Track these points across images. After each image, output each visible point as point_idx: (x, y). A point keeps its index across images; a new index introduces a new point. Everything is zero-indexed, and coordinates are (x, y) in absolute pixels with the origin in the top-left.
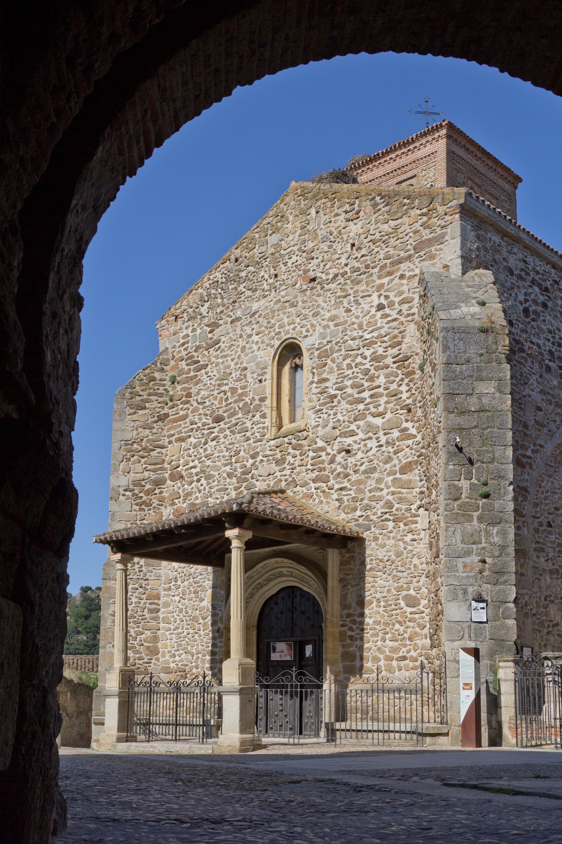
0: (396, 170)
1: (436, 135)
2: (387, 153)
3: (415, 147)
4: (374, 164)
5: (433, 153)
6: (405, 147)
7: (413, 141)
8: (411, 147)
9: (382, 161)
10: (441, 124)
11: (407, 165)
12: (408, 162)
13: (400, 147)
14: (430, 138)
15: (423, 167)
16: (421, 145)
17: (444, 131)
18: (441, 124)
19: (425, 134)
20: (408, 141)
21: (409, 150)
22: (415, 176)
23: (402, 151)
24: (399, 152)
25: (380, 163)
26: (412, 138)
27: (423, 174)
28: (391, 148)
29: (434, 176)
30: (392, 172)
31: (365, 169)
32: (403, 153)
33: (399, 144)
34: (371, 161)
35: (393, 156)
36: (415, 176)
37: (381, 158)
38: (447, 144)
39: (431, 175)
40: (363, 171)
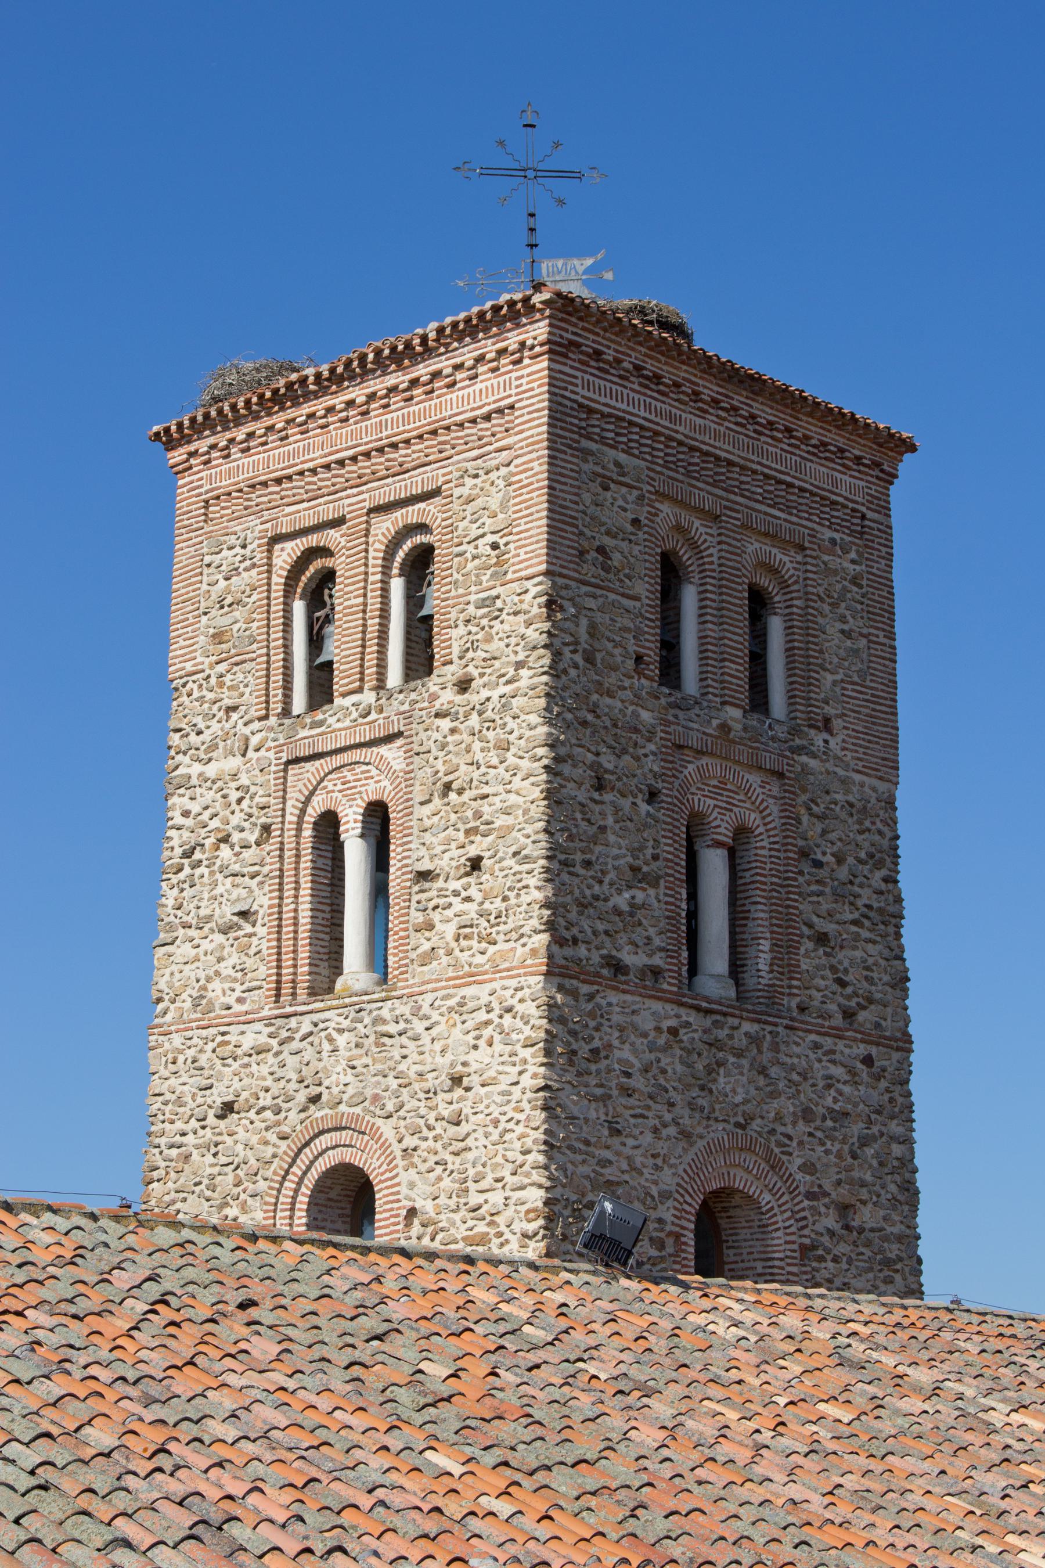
0: (367, 455)
1: (512, 340)
2: (335, 380)
3: (436, 375)
4: (291, 413)
5: (500, 411)
6: (400, 367)
7: (428, 351)
8: (422, 371)
9: (318, 406)
10: (526, 300)
11: (407, 442)
12: (412, 429)
13: (381, 364)
14: (489, 347)
15: (462, 460)
16: (458, 367)
17: (538, 331)
18: (526, 300)
19: (469, 330)
20: (408, 345)
21: (414, 383)
22: (435, 493)
23: (391, 380)
24: (378, 384)
25: (311, 416)
26: (424, 339)
27: (465, 491)
28: (348, 363)
29: (504, 506)
30: (354, 459)
31: (258, 427)
32: (393, 390)
33: (378, 352)
34: (279, 400)
35: (357, 393)
36: (435, 493)
37: (316, 395)
38: (554, 383)
39: (494, 503)
40: (251, 435)
